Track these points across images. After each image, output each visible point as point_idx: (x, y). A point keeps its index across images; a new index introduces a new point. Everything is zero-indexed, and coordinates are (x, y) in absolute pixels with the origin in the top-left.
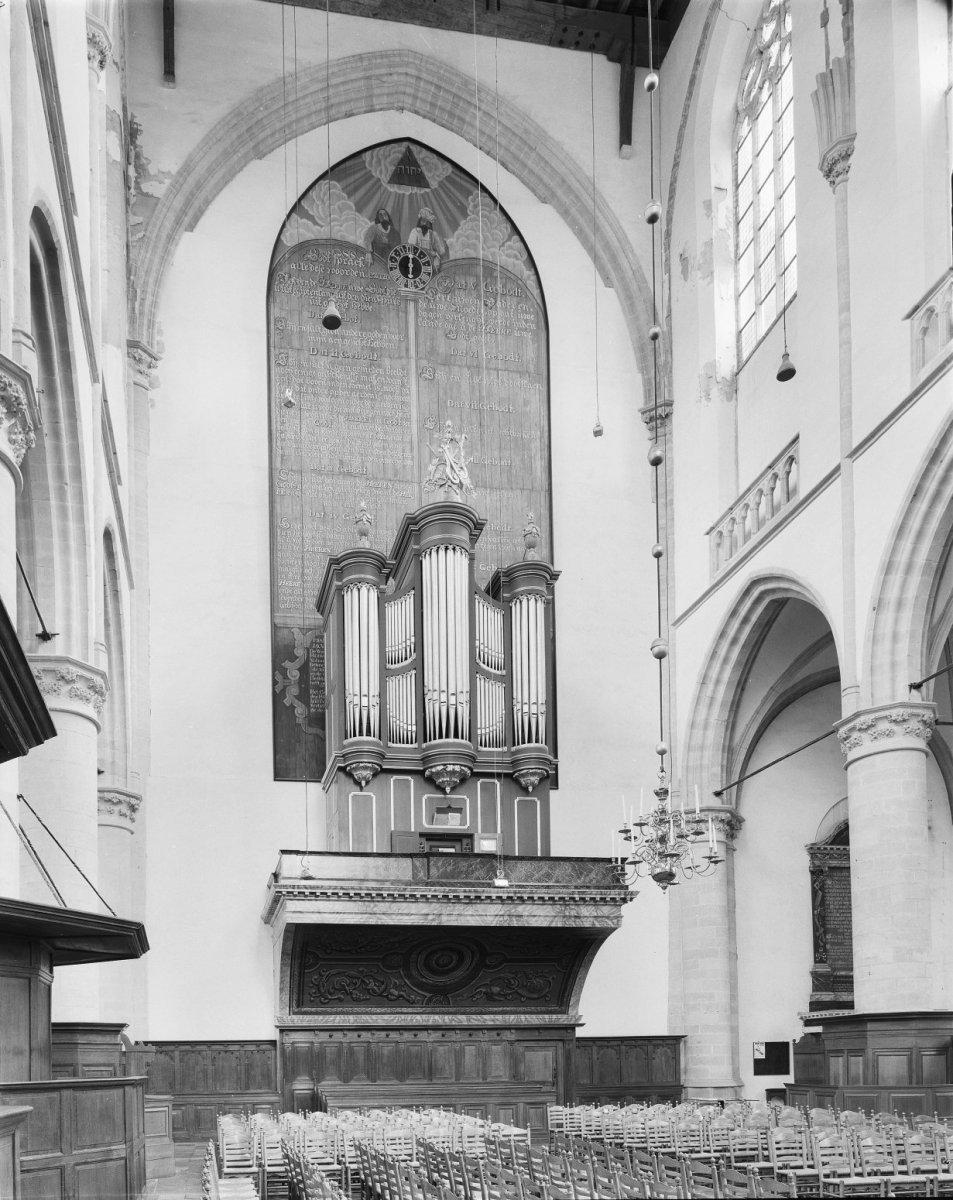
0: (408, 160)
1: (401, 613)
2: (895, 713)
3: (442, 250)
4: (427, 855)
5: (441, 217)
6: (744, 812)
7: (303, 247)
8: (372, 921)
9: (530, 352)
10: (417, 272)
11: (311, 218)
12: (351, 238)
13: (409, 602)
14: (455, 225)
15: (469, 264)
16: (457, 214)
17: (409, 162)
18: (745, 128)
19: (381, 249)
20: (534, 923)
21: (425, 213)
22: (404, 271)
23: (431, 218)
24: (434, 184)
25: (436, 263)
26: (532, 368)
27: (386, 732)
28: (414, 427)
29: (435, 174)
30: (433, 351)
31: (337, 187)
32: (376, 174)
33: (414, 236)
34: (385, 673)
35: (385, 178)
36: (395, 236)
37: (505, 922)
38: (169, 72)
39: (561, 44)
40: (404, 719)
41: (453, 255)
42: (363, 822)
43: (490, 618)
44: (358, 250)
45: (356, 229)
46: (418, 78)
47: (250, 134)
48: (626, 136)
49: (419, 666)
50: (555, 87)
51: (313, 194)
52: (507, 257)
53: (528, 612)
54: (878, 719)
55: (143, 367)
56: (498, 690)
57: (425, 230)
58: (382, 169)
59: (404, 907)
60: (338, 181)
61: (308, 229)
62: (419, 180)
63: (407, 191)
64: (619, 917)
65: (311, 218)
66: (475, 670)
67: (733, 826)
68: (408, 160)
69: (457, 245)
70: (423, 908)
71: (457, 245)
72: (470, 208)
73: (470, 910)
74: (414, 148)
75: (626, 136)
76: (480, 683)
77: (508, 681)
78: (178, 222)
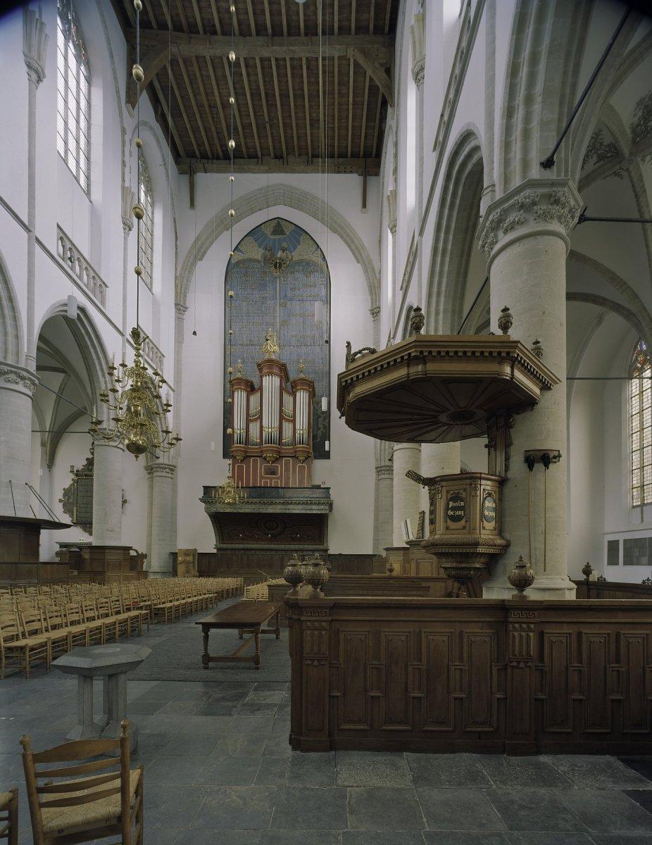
0: (279, 225)
3: (290, 257)
5: (291, 247)
8: (235, 511)
9: (323, 292)
11: (241, 252)
12: (256, 257)
14: (295, 248)
15: (300, 262)
16: (296, 244)
17: (279, 226)
21: (285, 245)
23: (286, 246)
24: (288, 233)
25: (288, 263)
26: (324, 299)
28: (278, 325)
29: (288, 230)
30: (286, 296)
31: (250, 239)
32: (266, 232)
33: (279, 254)
35: (269, 234)
36: (273, 255)
39: (339, 172)
41: (294, 260)
44: (258, 261)
45: (256, 253)
46: (285, 193)
47: (224, 223)
48: (364, 206)
50: (334, 188)
51: (242, 242)
52: (316, 258)
55: (181, 312)
58: (268, 231)
60: (252, 236)
61: (240, 255)
62: (282, 233)
63: (277, 237)
65: (241, 252)
68: (279, 225)
69: (296, 255)
71: (296, 255)
72: (301, 241)
74: (280, 220)
75: (364, 206)
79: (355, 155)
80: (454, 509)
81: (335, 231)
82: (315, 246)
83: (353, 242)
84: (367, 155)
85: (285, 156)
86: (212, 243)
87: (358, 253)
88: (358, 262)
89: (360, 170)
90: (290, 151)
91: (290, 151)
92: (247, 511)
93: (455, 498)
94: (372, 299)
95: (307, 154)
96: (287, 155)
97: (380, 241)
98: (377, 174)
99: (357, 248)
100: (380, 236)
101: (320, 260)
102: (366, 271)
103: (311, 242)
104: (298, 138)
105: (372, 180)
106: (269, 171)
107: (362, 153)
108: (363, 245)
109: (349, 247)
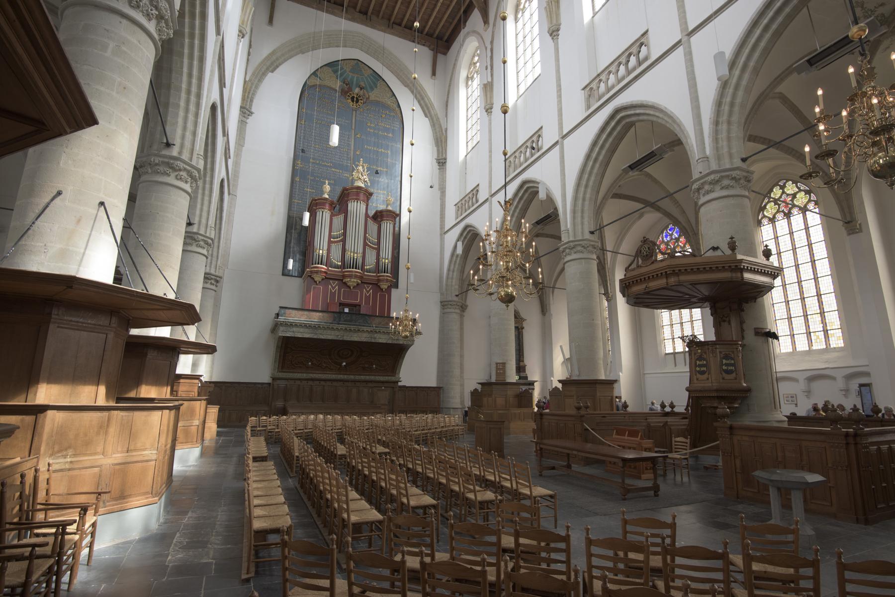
1: (338, 220)
2: (734, 174)
4: (339, 313)
6: (468, 303)
7: (314, 86)
8: (315, 337)
10: (357, 102)
13: (342, 217)
14: (372, 89)
17: (358, 64)
18: (470, 83)
19: (344, 92)
20: (380, 341)
21: (362, 84)
22: (353, 101)
27: (329, 263)
31: (330, 70)
33: (357, 90)
34: (330, 242)
36: (350, 89)
37: (369, 340)
38: (271, 21)
40: (336, 259)
42: (316, 298)
43: (373, 227)
45: (337, 85)
49: (344, 241)
52: (389, 102)
53: (387, 227)
54: (722, 177)
56: (374, 252)
57: (361, 89)
59: (329, 332)
64: (413, 341)
66: (365, 244)
67: (463, 308)
69: (373, 95)
70: (337, 333)
73: (356, 335)
75: (434, 73)
76: (368, 249)
77: (378, 250)
78: (267, 69)
79: (429, 35)
80: (726, 365)
81: (406, 86)
82: (391, 94)
83: (423, 99)
84: (439, 38)
85: (369, 14)
86: (285, 60)
87: (427, 110)
88: (426, 116)
89: (432, 47)
90: (377, 12)
91: (377, 12)
92: (330, 337)
93: (726, 357)
94: (438, 150)
95: (389, 20)
96: (372, 13)
97: (447, 106)
98: (445, 54)
99: (426, 105)
100: (447, 102)
101: (395, 106)
102: (433, 125)
103: (387, 89)
104: (387, 7)
105: (440, 57)
106: (353, 19)
107: (435, 35)
108: (432, 105)
109: (419, 102)
